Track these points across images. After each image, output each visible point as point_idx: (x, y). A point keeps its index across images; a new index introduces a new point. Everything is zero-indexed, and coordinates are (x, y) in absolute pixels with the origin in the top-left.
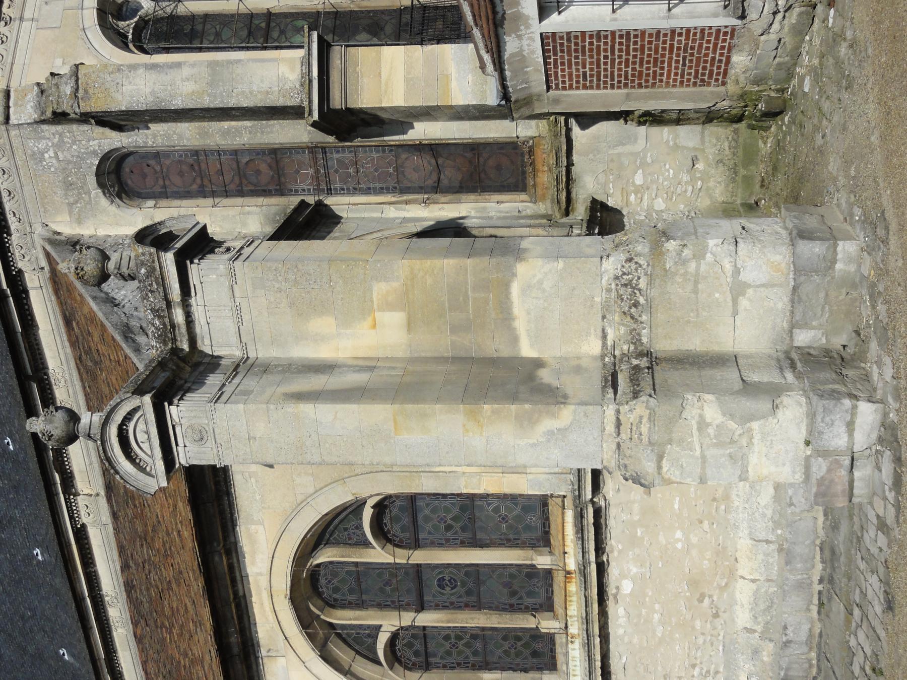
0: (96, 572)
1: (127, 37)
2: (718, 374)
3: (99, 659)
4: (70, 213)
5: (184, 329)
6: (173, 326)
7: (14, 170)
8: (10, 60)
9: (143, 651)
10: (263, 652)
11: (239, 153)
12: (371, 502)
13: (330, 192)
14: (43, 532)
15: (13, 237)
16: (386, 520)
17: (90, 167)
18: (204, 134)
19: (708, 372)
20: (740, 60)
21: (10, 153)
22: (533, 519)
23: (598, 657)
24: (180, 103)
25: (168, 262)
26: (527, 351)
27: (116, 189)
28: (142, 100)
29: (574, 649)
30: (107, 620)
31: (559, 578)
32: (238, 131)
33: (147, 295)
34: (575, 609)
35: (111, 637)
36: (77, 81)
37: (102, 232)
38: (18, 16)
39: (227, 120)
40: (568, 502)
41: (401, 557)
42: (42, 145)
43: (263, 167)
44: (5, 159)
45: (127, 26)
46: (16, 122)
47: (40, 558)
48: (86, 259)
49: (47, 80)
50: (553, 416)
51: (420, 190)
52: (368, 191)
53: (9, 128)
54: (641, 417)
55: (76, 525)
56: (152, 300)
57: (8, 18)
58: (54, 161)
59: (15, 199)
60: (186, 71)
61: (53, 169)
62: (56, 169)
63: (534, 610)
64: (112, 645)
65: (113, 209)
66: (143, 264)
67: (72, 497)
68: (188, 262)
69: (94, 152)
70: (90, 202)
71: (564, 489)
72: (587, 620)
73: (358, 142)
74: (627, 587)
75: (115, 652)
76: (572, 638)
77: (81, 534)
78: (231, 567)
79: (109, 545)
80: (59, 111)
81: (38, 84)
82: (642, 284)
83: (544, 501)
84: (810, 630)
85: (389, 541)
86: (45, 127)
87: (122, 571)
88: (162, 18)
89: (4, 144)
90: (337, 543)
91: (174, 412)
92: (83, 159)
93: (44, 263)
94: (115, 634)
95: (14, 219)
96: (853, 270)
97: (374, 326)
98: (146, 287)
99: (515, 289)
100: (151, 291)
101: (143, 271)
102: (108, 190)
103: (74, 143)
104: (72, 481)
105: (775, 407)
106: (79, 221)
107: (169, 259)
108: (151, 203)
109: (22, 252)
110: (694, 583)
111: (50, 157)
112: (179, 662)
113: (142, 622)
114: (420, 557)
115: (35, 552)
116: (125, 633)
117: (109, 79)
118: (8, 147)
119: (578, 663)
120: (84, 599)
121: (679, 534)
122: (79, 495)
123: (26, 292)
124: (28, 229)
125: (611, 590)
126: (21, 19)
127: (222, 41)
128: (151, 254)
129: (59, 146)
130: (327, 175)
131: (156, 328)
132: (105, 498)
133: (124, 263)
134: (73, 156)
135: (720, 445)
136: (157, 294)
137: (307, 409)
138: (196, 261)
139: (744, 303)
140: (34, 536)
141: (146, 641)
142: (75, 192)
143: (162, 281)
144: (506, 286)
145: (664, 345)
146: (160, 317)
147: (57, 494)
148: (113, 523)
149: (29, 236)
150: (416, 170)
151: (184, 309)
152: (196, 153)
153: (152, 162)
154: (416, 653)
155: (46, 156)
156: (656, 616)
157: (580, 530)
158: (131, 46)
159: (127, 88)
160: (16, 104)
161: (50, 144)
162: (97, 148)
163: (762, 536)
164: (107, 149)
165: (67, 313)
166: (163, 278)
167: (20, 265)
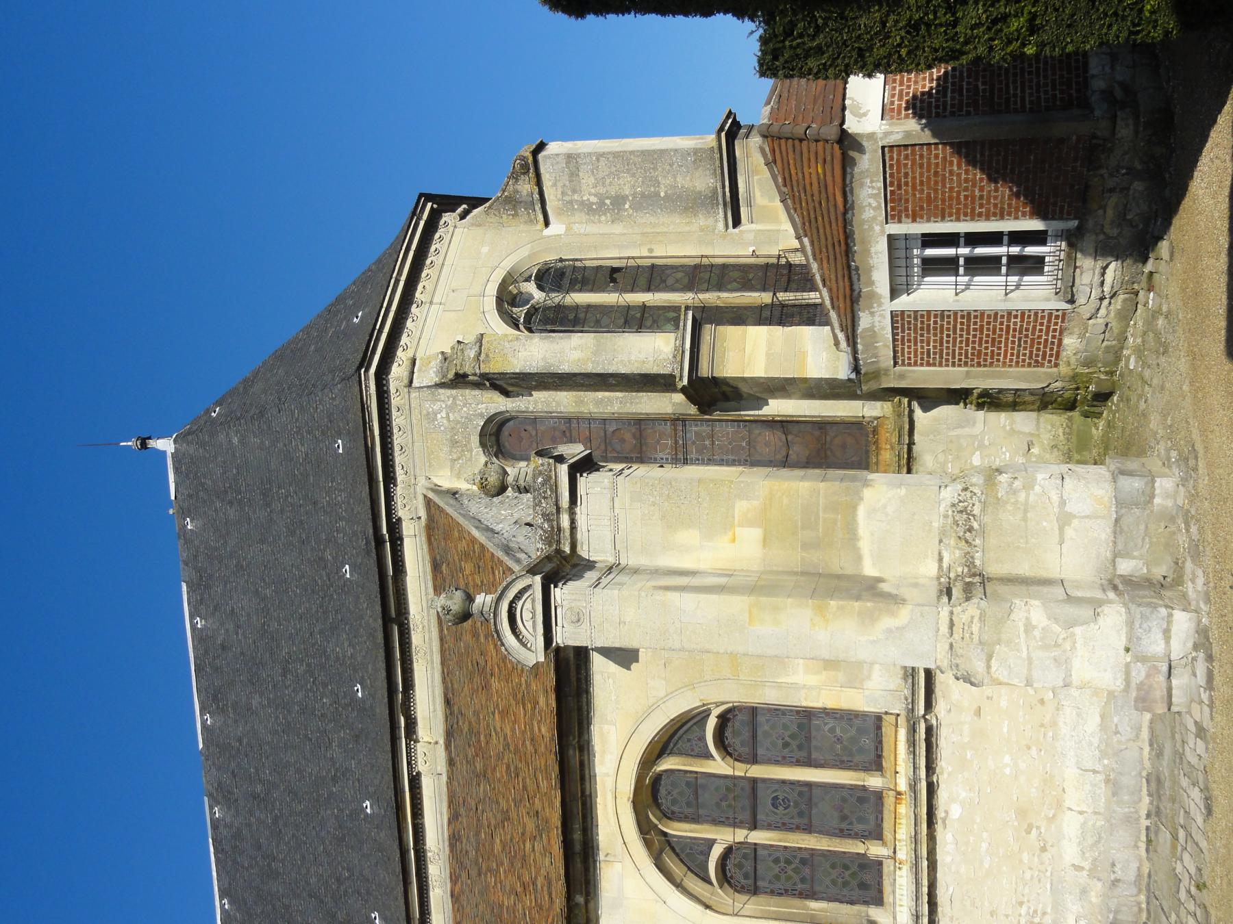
0: (423, 824)
1: (519, 321)
2: (1045, 590)
3: (413, 918)
4: (452, 469)
5: (567, 533)
6: (559, 529)
7: (409, 428)
8: (418, 336)
9: (458, 910)
10: (602, 856)
11: (607, 422)
12: (716, 712)
14: (376, 782)
15: (398, 488)
16: (728, 733)
17: (476, 428)
18: (580, 402)
19: (1035, 588)
20: (1071, 342)
21: (408, 412)
22: (867, 742)
23: (925, 882)
24: (566, 368)
25: (562, 473)
26: (869, 570)
27: (495, 450)
28: (534, 364)
29: (901, 877)
30: (427, 878)
31: (889, 800)
32: (610, 400)
33: (540, 501)
34: (904, 832)
35: (428, 897)
36: (481, 347)
38: (429, 300)
39: (602, 390)
40: (902, 721)
41: (740, 770)
43: (628, 436)
44: (403, 417)
45: (520, 312)
46: (418, 385)
47: (368, 811)
48: (491, 472)
49: (453, 348)
50: (892, 614)
51: (770, 463)
52: (721, 463)
53: (411, 390)
54: (972, 617)
55: (412, 772)
56: (544, 505)
57: (420, 302)
58: (445, 422)
59: (406, 454)
61: (442, 428)
62: (445, 428)
63: (864, 836)
64: (427, 906)
66: (540, 473)
67: (412, 743)
68: (578, 475)
69: (481, 415)
70: (470, 460)
71: (899, 708)
72: (916, 840)
73: (717, 415)
74: (955, 811)
75: (429, 914)
76: (900, 864)
77: (415, 781)
78: (582, 764)
79: (440, 795)
80: (461, 372)
81: (443, 353)
82: (977, 511)
83: (878, 719)
84: (1139, 868)
85: (730, 755)
86: (442, 391)
87: (449, 822)
88: (551, 307)
89: (405, 404)
90: (680, 753)
91: (558, 593)
92: (470, 420)
93: (422, 513)
94: (431, 894)
95: (402, 472)
96: (1171, 505)
97: (734, 540)
98: (540, 494)
99: (861, 512)
100: (545, 498)
101: (540, 480)
102: (488, 450)
103: (465, 405)
104: (414, 728)
105: (1096, 615)
107: (563, 469)
109: (404, 502)
110: (1022, 813)
111: (442, 417)
112: (501, 906)
113: (464, 875)
114: (757, 771)
115: (365, 805)
116: (442, 893)
117: (508, 346)
118: (407, 407)
119: (905, 893)
120: (408, 851)
121: (1007, 759)
122: (419, 742)
123: (401, 539)
124: (413, 481)
125: (940, 814)
126: (431, 303)
127: (601, 327)
128: (549, 464)
129: (451, 408)
130: (685, 446)
131: (544, 531)
132: (443, 747)
133: (522, 476)
134: (462, 417)
135: (1045, 647)
136: (550, 499)
137: (673, 596)
138: (585, 475)
139: (1069, 532)
140: (367, 787)
141: (463, 899)
142: (460, 449)
143: (555, 489)
144: (854, 508)
145: (993, 569)
146: (549, 520)
147: (400, 738)
148: (448, 771)
149: (413, 487)
150: (767, 444)
151: (570, 516)
153: (529, 428)
154: (746, 876)
155: (439, 416)
156: (984, 845)
157: (912, 743)
158: (521, 327)
159: (523, 354)
160: (420, 370)
161: (444, 406)
162: (484, 411)
163: (1089, 765)
164: (493, 412)
165: (438, 558)
166: (556, 486)
167: (401, 513)
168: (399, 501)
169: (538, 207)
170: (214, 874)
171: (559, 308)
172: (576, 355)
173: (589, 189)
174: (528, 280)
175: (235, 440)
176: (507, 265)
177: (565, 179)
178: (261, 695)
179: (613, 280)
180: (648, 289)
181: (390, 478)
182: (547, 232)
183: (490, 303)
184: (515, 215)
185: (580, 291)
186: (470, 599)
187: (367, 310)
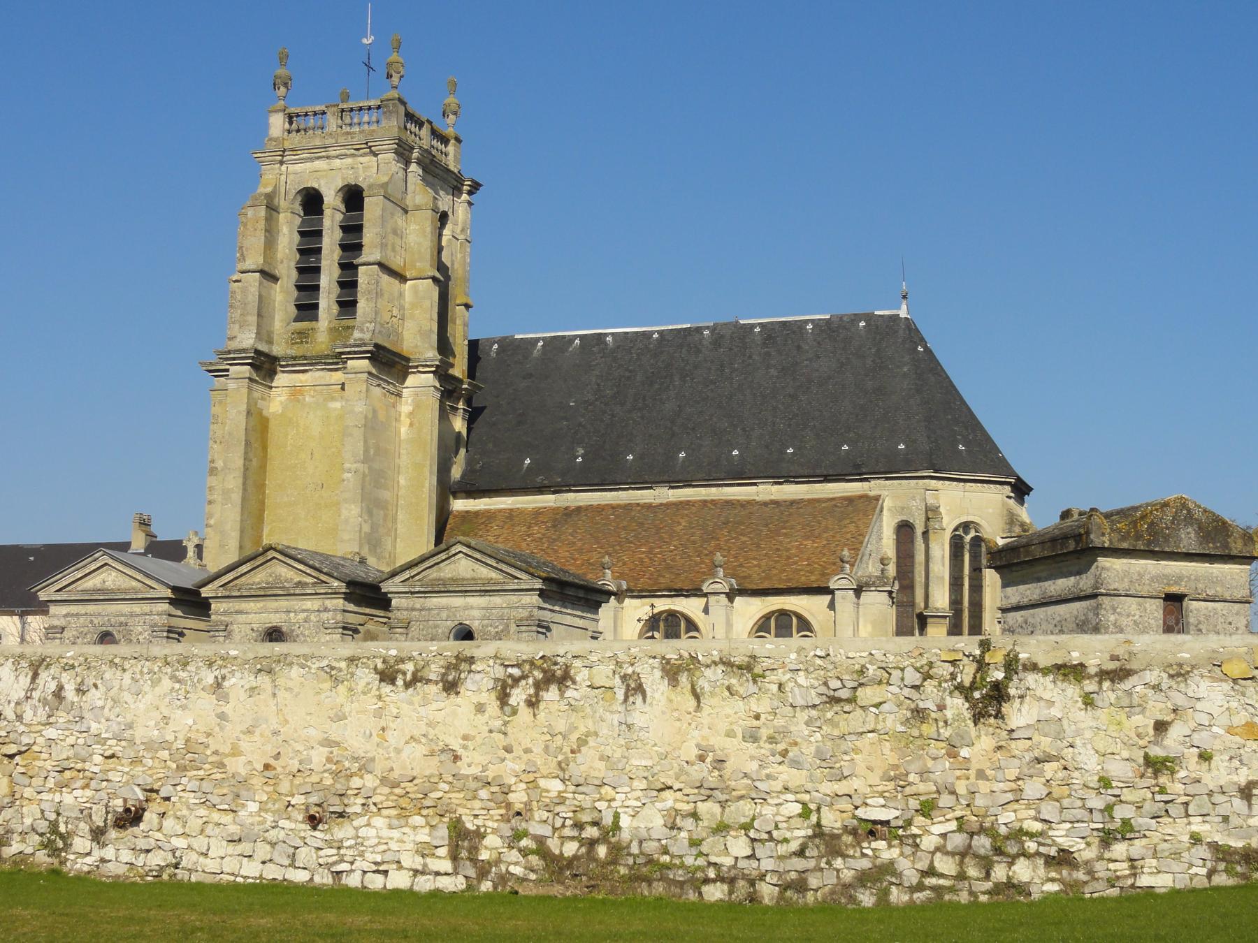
13: (897, 606)
32: (920, 577)
37: (884, 518)
42: (918, 501)
45: (960, 532)
52: (897, 620)
60: (941, 568)
65: (893, 524)
73: (916, 620)
77: (755, 484)
87: (738, 501)
106: (889, 510)
108: (895, 537)
143: (883, 586)
168: (878, 482)
169: (1009, 535)
170: (670, 327)
171: (963, 547)
172: (936, 569)
174: (976, 531)
175: (905, 369)
178: (778, 377)
179: (975, 570)
180: (970, 586)
181: (887, 479)
182: (998, 538)
183: (964, 519)
184: (1006, 523)
185: (970, 556)
186: (847, 562)
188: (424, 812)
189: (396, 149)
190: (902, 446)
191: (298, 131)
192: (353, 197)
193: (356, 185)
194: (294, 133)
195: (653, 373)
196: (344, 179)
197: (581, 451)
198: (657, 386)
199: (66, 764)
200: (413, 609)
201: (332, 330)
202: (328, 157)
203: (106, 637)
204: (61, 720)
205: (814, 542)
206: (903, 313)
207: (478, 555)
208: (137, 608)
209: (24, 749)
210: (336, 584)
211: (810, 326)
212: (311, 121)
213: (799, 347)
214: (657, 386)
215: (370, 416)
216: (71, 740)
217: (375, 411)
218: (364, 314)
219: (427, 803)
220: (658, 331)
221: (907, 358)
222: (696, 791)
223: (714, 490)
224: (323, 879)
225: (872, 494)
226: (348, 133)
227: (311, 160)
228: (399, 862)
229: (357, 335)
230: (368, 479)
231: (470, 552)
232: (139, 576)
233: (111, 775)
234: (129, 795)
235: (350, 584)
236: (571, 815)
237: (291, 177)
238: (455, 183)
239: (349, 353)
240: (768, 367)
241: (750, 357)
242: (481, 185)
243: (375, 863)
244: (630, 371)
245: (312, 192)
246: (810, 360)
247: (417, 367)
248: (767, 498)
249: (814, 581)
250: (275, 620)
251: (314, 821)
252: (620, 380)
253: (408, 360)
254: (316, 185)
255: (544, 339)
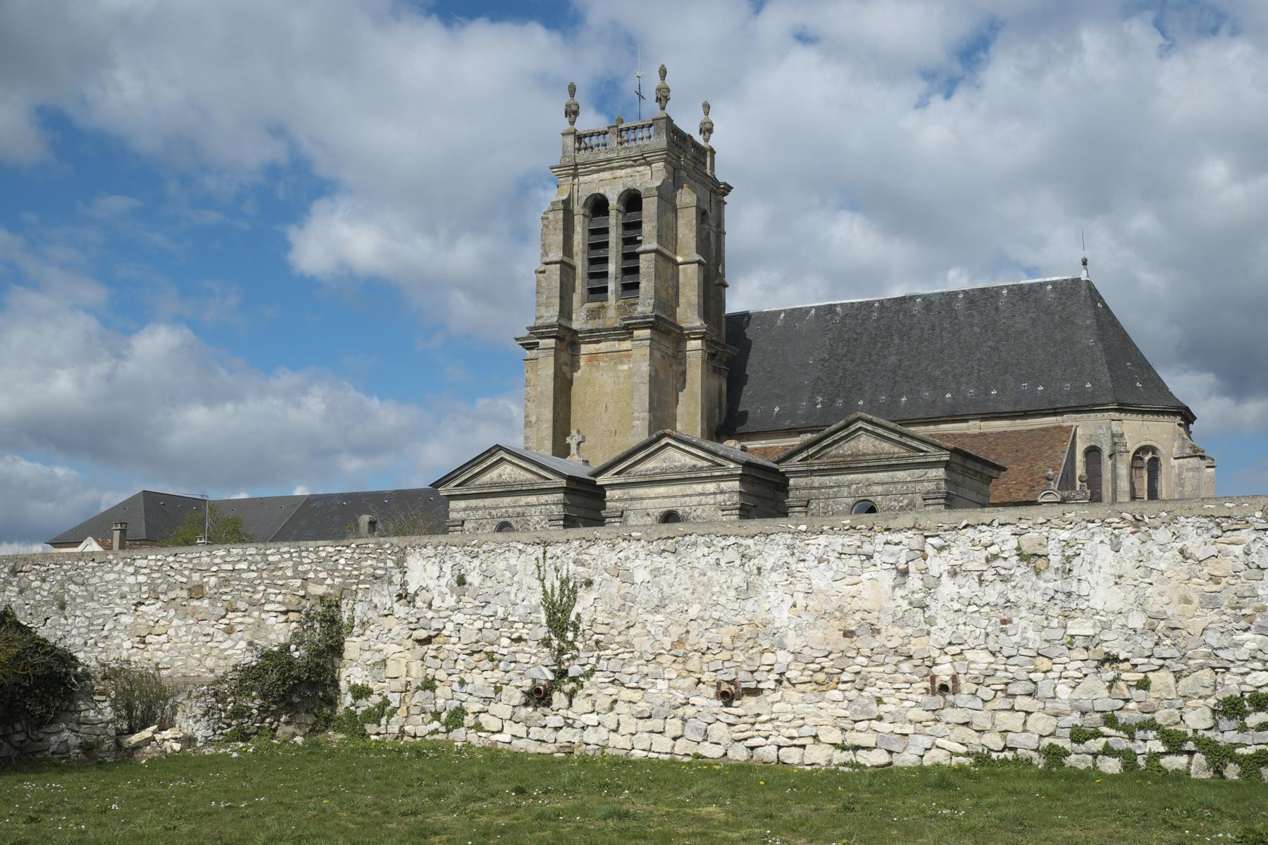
87: (952, 435)
152: (1101, 476)
159: (1122, 467)
167: (1065, 416)
172: (1122, 485)
173: (1186, 475)
176: (1159, 446)
177: (1190, 466)
178: (981, 333)
182: (1172, 458)
187: (1141, 389)
188: (841, 686)
189: (665, 158)
190: (1088, 385)
191: (586, 149)
192: (632, 201)
193: (634, 190)
194: (583, 151)
195: (876, 334)
196: (623, 184)
197: (820, 399)
198: (880, 345)
199: (475, 647)
200: (814, 488)
201: (619, 308)
202: (612, 169)
203: (503, 527)
204: (469, 606)
205: (1019, 465)
206: (1084, 277)
207: (880, 431)
208: (532, 499)
209: (433, 633)
210: (732, 465)
211: (1005, 292)
212: (594, 140)
213: (997, 309)
214: (880, 345)
215: (653, 374)
216: (479, 624)
217: (656, 371)
218: (646, 291)
219: (844, 677)
220: (878, 301)
221: (1089, 313)
222: (1146, 660)
223: (931, 427)
224: (739, 754)
225: (1065, 424)
226: (627, 148)
227: (598, 172)
228: (815, 737)
229: (640, 309)
230: (653, 425)
231: (870, 428)
232: (534, 469)
233: (519, 657)
234: (537, 675)
235: (747, 465)
236: (1002, 687)
237: (582, 186)
238: (712, 187)
239: (635, 324)
240: (972, 325)
241: (956, 318)
242: (731, 188)
243: (792, 738)
244: (857, 334)
245: (599, 197)
246: (1007, 318)
247: (688, 334)
248: (977, 431)
249: (1021, 496)
250: (668, 505)
251: (727, 698)
252: (849, 341)
253: (681, 329)
254: (601, 191)
255: (785, 311)
